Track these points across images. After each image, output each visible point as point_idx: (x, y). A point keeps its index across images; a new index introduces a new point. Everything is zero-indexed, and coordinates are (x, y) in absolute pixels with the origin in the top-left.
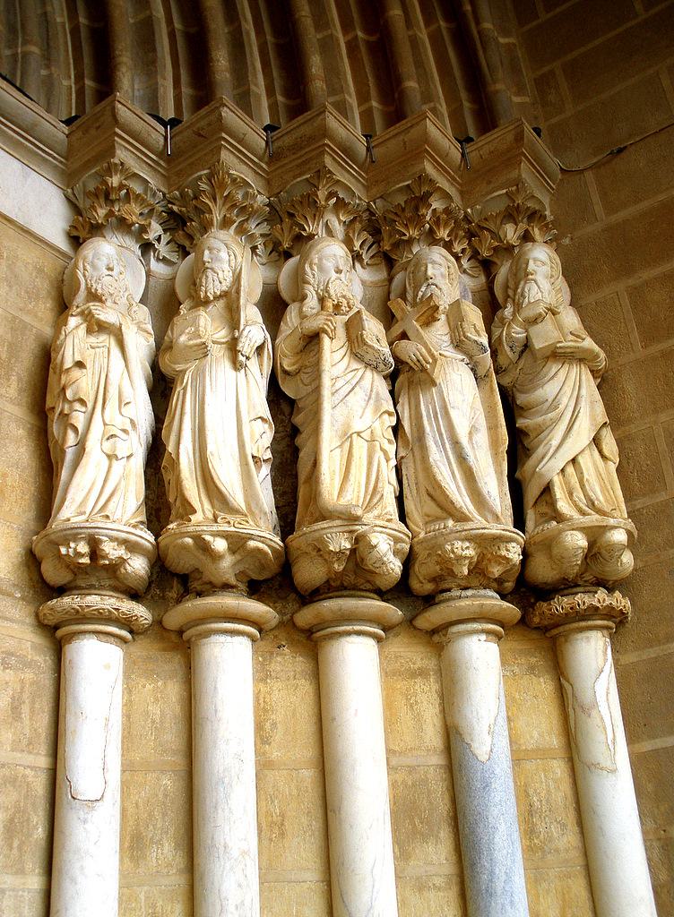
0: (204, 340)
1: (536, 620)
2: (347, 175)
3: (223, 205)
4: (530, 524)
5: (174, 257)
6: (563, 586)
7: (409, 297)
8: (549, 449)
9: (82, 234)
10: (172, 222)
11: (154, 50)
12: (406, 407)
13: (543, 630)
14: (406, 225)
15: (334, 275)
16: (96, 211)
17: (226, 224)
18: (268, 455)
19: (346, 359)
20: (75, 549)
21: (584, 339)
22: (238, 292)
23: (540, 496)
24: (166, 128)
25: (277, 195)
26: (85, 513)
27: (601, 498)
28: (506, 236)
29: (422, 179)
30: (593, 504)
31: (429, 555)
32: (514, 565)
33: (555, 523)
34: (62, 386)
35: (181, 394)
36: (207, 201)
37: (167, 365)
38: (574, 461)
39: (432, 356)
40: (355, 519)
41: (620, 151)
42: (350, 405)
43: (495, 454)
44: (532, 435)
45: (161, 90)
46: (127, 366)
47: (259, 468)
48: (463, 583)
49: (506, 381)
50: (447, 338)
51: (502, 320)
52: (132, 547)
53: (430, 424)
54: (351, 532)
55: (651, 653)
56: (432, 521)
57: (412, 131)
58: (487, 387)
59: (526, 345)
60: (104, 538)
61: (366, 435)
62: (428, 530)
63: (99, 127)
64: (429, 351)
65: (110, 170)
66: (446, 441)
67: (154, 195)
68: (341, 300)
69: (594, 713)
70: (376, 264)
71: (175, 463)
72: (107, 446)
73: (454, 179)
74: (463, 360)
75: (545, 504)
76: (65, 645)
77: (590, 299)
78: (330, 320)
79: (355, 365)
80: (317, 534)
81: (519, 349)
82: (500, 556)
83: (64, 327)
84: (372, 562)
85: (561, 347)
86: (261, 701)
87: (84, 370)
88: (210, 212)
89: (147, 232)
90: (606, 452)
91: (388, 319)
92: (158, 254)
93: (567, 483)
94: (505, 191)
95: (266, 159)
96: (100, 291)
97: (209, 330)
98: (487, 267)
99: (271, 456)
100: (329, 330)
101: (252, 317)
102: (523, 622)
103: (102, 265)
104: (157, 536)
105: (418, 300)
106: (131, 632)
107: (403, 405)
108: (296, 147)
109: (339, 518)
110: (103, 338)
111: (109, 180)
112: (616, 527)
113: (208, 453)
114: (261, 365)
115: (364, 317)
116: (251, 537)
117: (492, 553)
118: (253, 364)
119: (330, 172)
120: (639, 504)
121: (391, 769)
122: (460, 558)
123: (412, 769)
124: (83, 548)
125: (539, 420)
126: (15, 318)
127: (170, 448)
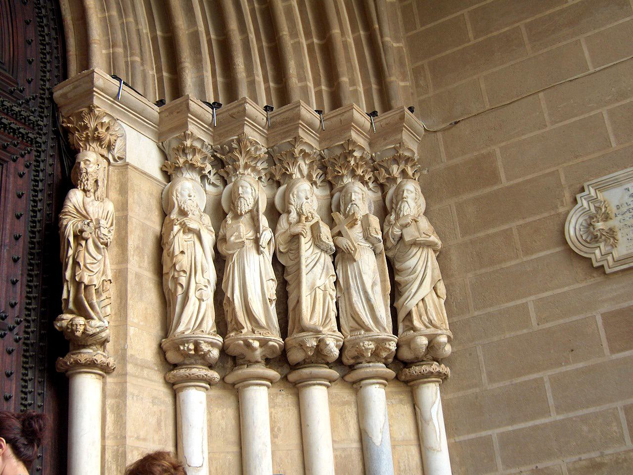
1: (403, 377)
2: (309, 137)
3: (246, 156)
4: (400, 331)
5: (218, 183)
7: (342, 209)
9: (170, 171)
11: (200, 53)
12: (341, 271)
13: (406, 382)
14: (340, 167)
15: (305, 201)
17: (246, 166)
18: (275, 297)
20: (188, 347)
21: (430, 236)
22: (258, 211)
24: (213, 109)
26: (190, 329)
27: (436, 319)
28: (393, 172)
29: (350, 141)
30: (431, 322)
31: (352, 347)
32: (393, 352)
33: (412, 332)
35: (232, 266)
36: (237, 155)
37: (222, 249)
38: (423, 300)
39: (354, 247)
40: (319, 332)
41: (456, 123)
42: (315, 273)
43: (384, 295)
44: (403, 285)
45: (206, 80)
46: (204, 251)
47: (271, 304)
48: (368, 360)
49: (390, 254)
50: (361, 235)
51: (389, 222)
52: (213, 345)
53: (353, 282)
54: (317, 338)
55: (461, 394)
57: (345, 115)
58: (381, 259)
59: (401, 237)
61: (322, 288)
63: (179, 112)
64: (353, 244)
65: (185, 137)
67: (207, 147)
69: (430, 423)
71: (231, 302)
72: (198, 293)
76: (179, 392)
77: (436, 207)
79: (317, 251)
80: (301, 339)
81: (397, 239)
82: (386, 348)
85: (418, 241)
86: (273, 417)
88: (239, 160)
89: (204, 170)
91: (332, 223)
93: (419, 311)
94: (393, 146)
95: (267, 127)
96: (186, 209)
98: (382, 187)
100: (304, 234)
101: (264, 221)
102: (397, 378)
103: (186, 193)
104: (224, 338)
106: (210, 384)
107: (339, 270)
108: (283, 123)
109: (312, 331)
110: (191, 235)
111: (185, 143)
112: (442, 334)
114: (269, 249)
115: (321, 225)
116: (271, 340)
119: (302, 138)
120: (455, 319)
121: (335, 449)
122: (367, 349)
123: (344, 450)
124: (192, 347)
125: (406, 278)
126: (143, 223)
127: (229, 295)
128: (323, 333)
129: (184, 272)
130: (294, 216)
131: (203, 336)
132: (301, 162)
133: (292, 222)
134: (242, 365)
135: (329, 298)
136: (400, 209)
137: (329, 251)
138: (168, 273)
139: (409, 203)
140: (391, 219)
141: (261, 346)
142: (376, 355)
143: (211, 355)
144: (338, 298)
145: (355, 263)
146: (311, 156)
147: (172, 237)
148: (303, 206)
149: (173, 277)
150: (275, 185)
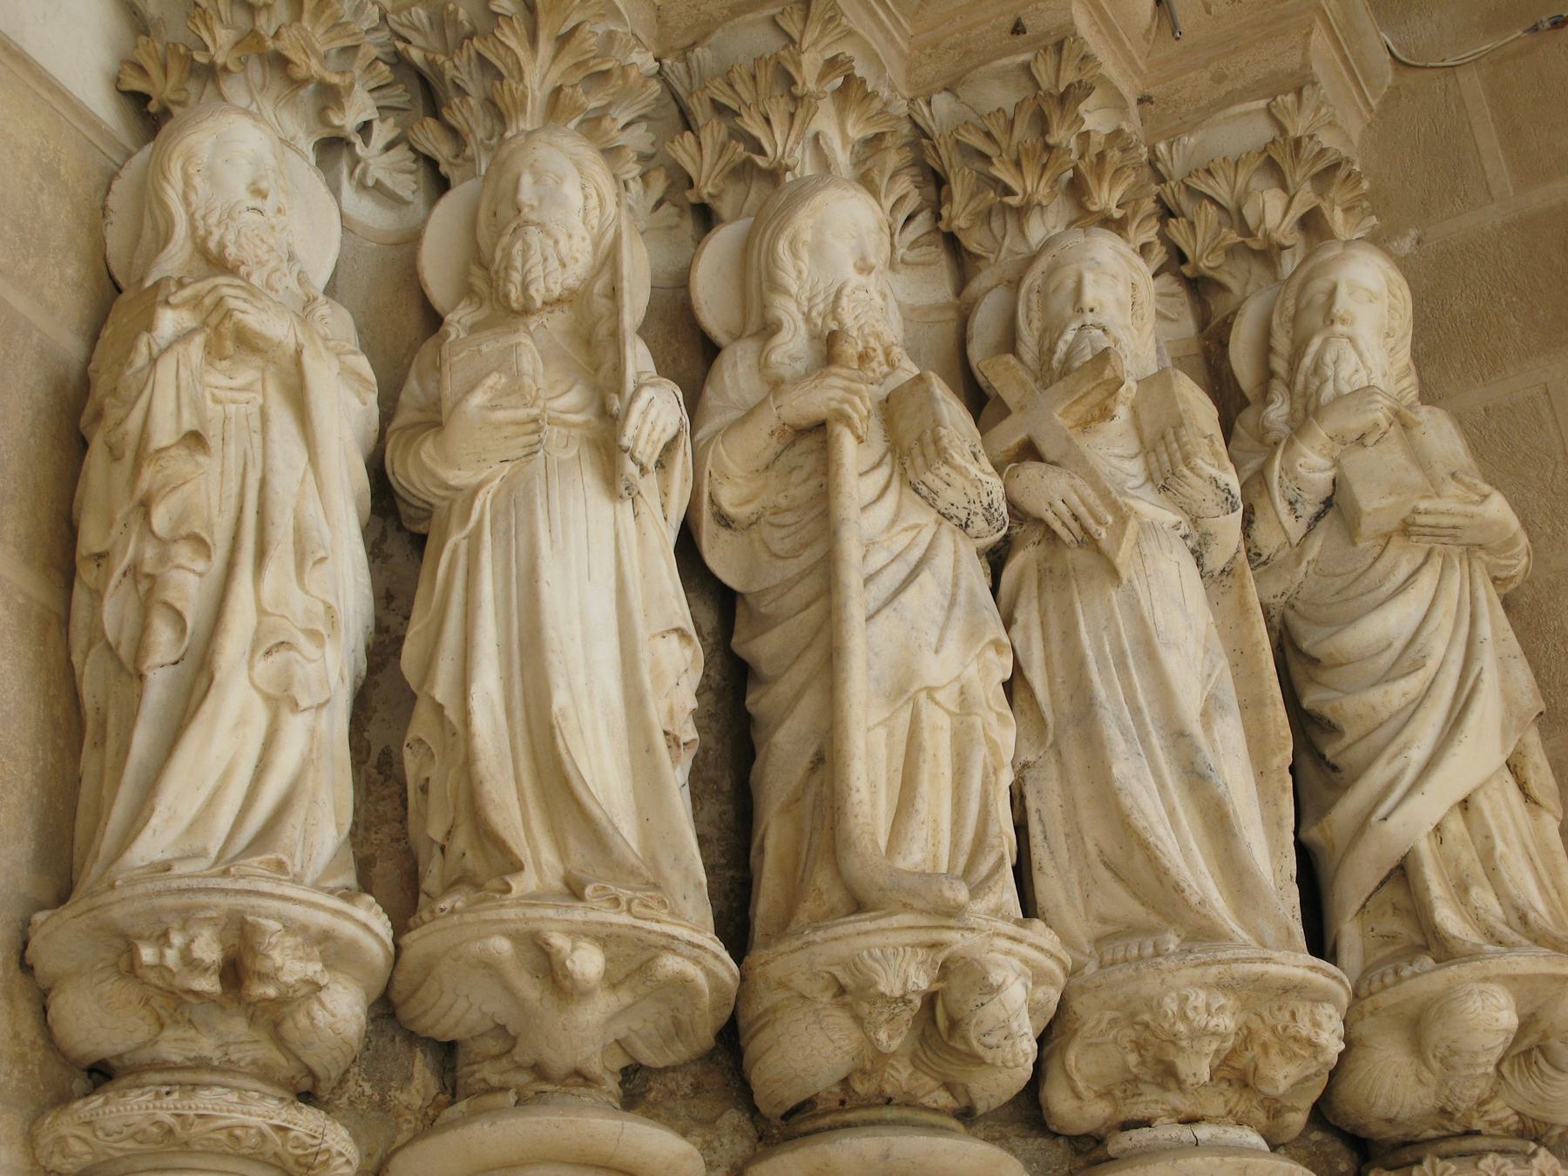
0: (535, 411)
3: (555, 58)
5: (407, 185)
6: (1432, 1133)
8: (1402, 771)
9: (162, 89)
10: (400, 89)
12: (1036, 635)
15: (854, 278)
16: (210, 30)
19: (891, 499)
21: (1485, 497)
23: (1377, 889)
25: (684, 54)
27: (1541, 906)
28: (1262, 220)
30: (1523, 918)
34: (138, 494)
38: (1465, 804)
39: (1115, 507)
50: (1135, 467)
51: (1261, 433)
53: (1108, 683)
54: (934, 946)
56: (1115, 936)
60: (272, 925)
61: (947, 697)
62: (1108, 958)
66: (1151, 728)
68: (873, 342)
70: (923, 264)
71: (458, 734)
73: (1131, 62)
74: (1176, 527)
75: (1390, 910)
78: (856, 392)
80: (842, 949)
83: (144, 338)
84: (985, 1028)
87: (201, 459)
89: (340, 106)
90: (1536, 792)
92: (364, 173)
96: (231, 252)
97: (542, 383)
99: (696, 736)
100: (855, 416)
104: (401, 927)
105: (1055, 364)
107: (1026, 628)
109: (907, 907)
113: (555, 708)
116: (670, 944)
117: (1274, 1030)
118: (649, 486)
124: (208, 950)
125: (1375, 696)
127: (442, 689)
128: (973, 921)
129: (200, 544)
130: (792, 345)
131: (278, 891)
132: (825, 121)
133: (786, 372)
134: (491, 1090)
135: (980, 755)
136: (1317, 368)
137: (979, 523)
138: (101, 557)
139: (1362, 344)
140: (1272, 416)
141: (612, 983)
143: (321, 1016)
144: (1022, 770)
145: (1115, 595)
146: (877, 105)
147: (141, 358)
148: (844, 302)
149: (134, 571)
150: (688, 225)
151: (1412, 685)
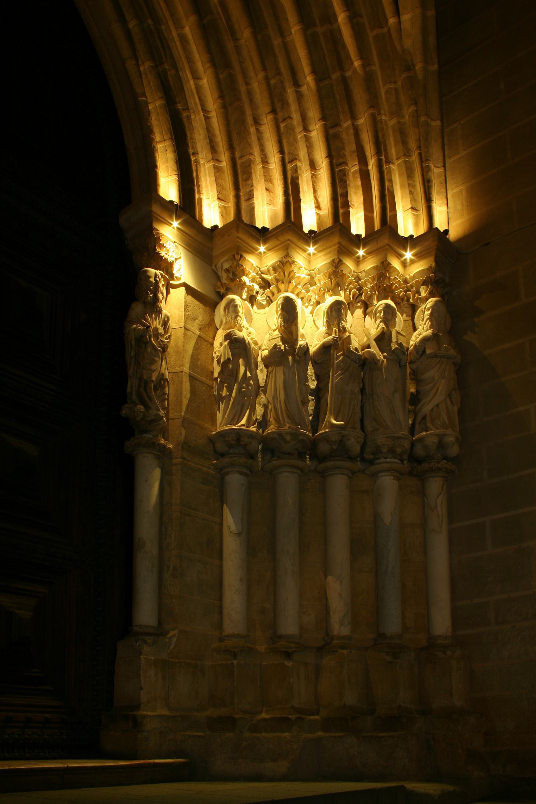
23: (421, 421)
38: (438, 405)
41: (487, 244)
54: (340, 433)
81: (421, 353)
142: (392, 451)
151: (431, 385)
